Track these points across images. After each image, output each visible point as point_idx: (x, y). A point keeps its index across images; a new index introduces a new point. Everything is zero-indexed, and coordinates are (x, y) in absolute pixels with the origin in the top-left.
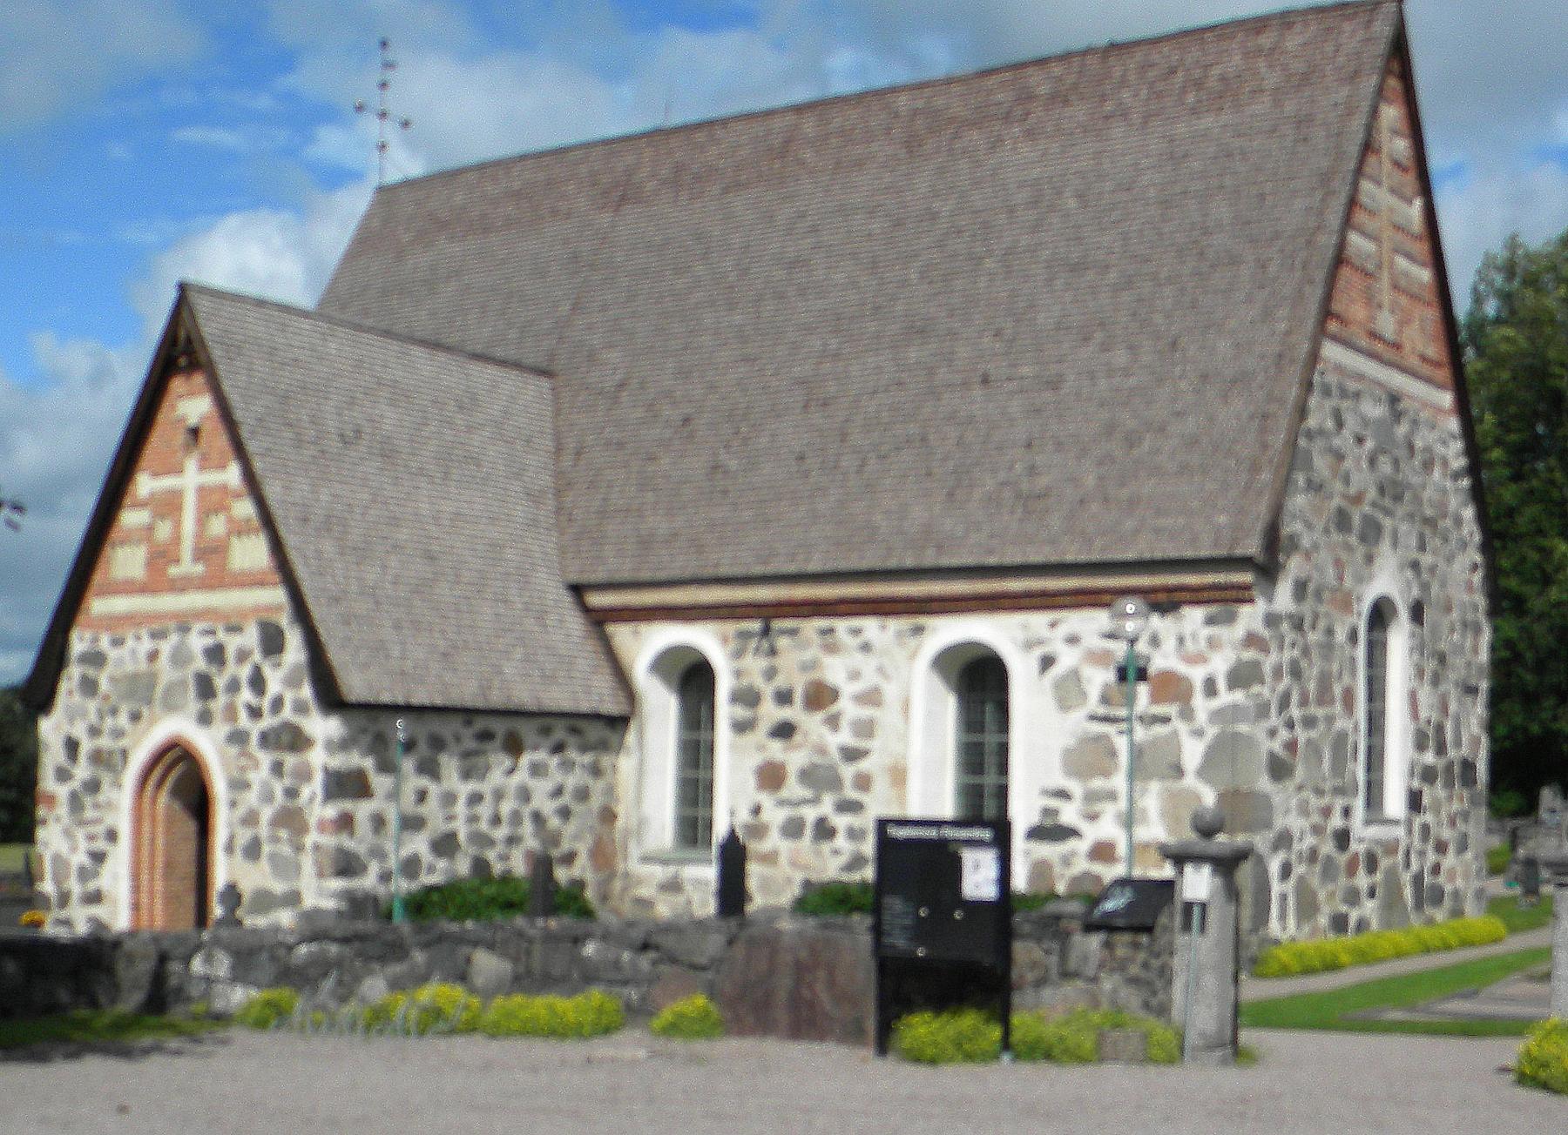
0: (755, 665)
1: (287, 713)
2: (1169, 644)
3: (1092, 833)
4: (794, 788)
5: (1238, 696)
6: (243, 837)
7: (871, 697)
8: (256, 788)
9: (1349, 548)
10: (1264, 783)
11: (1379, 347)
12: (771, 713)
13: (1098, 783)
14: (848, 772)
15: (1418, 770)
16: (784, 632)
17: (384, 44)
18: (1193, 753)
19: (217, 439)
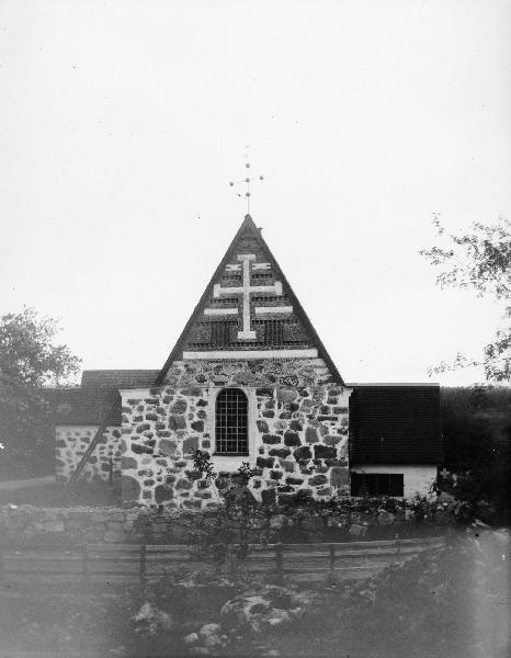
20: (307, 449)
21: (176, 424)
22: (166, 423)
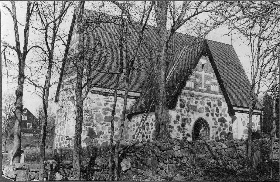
1: (223, 116)
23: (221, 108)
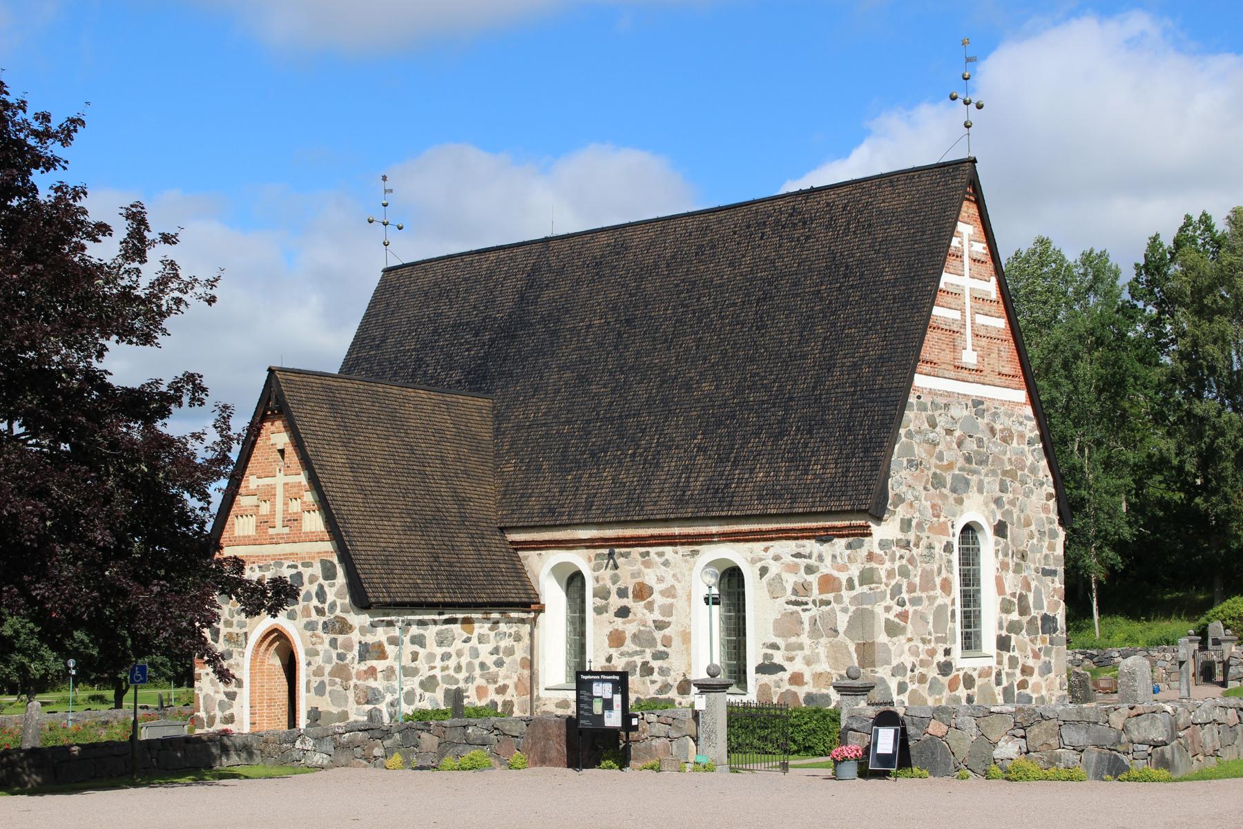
0: (606, 574)
1: (338, 612)
2: (828, 560)
3: (791, 668)
4: (629, 646)
5: (865, 588)
6: (315, 681)
7: (670, 592)
8: (322, 653)
9: (944, 497)
10: (882, 638)
11: (964, 374)
12: (615, 602)
13: (793, 639)
14: (658, 635)
15: (1005, 625)
16: (622, 555)
17: (384, 178)
18: (842, 622)
19: (292, 457)
20: (1035, 618)
21: (927, 583)
22: (917, 580)
23: (332, 585)
